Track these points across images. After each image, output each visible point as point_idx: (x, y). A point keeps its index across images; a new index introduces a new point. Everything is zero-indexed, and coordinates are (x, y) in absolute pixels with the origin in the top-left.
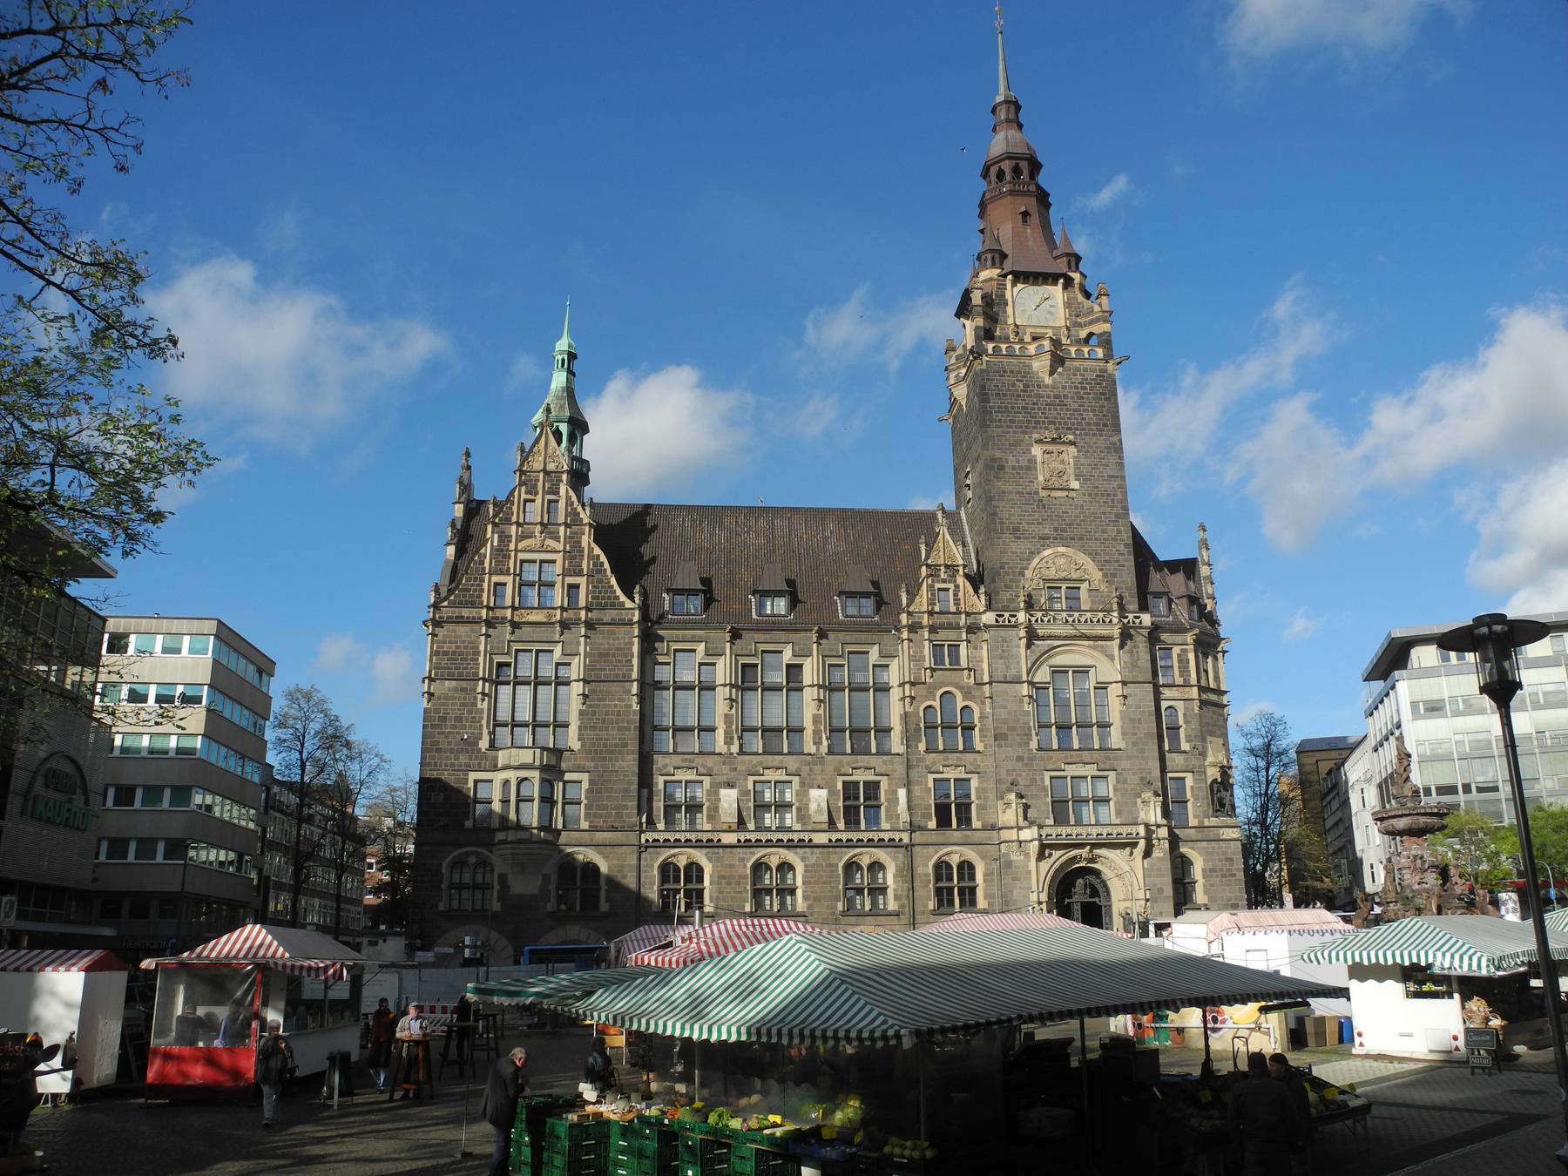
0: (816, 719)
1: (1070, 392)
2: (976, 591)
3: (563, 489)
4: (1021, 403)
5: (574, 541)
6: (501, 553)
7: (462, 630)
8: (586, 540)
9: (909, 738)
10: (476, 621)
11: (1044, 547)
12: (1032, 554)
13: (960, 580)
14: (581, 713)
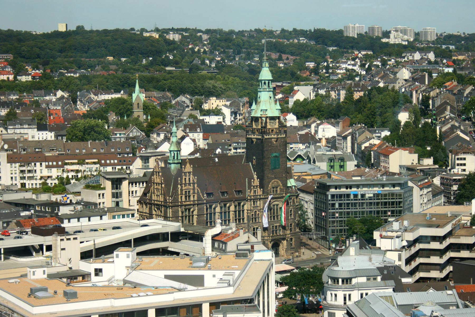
0: (233, 217)
1: (278, 145)
2: (261, 189)
3: (191, 176)
4: (270, 148)
5: (194, 186)
6: (182, 190)
7: (176, 208)
8: (196, 185)
9: (248, 220)
10: (178, 206)
11: (273, 180)
12: (270, 182)
13: (258, 188)
14: (197, 221)
